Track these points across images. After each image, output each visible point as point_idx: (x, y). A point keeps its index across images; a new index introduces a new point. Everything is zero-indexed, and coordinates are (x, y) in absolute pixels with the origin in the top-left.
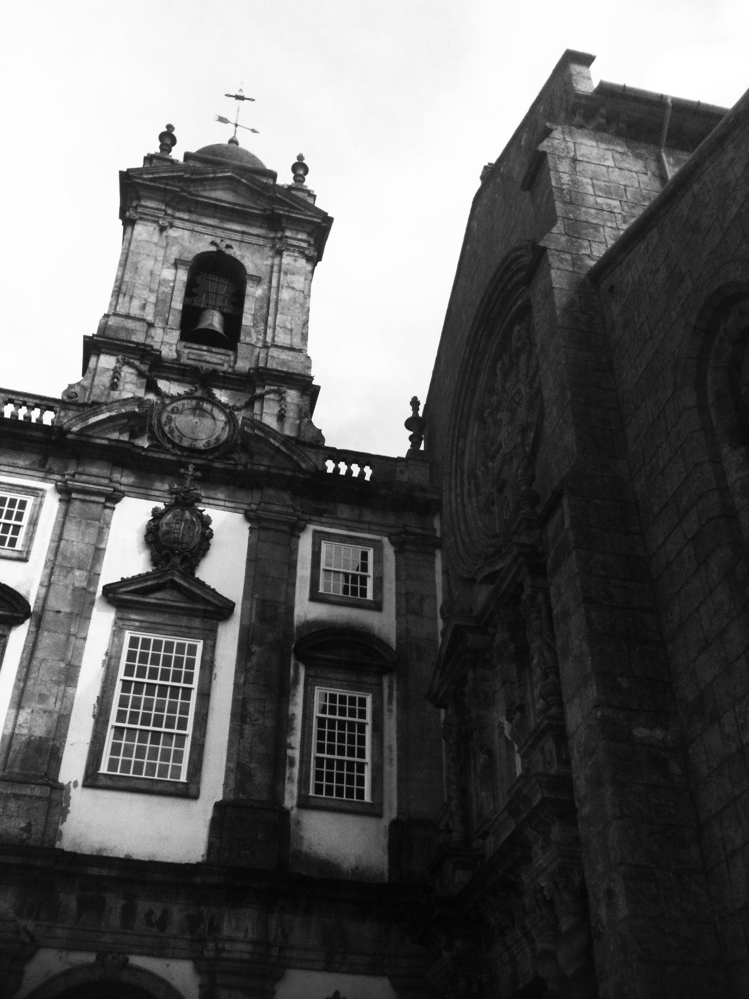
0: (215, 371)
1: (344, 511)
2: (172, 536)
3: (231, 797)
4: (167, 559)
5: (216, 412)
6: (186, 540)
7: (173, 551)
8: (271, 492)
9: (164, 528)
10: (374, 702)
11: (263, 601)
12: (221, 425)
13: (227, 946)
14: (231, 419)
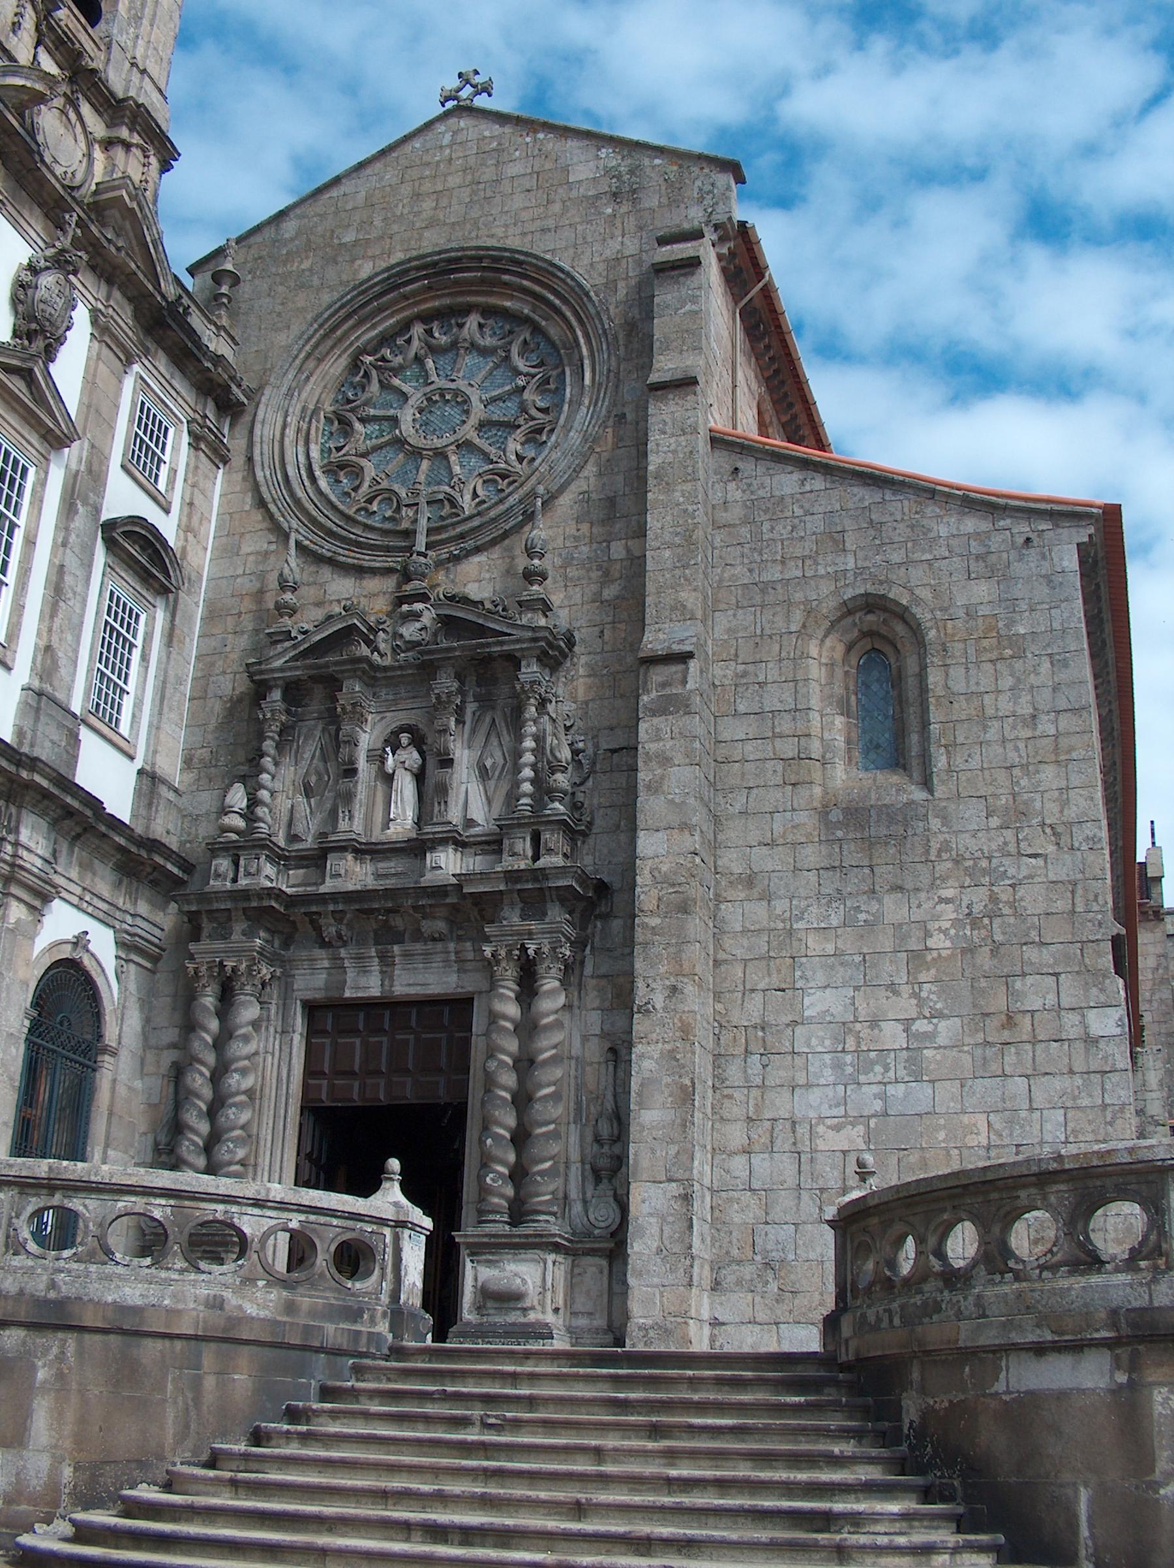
0: (94, 71)
1: (162, 362)
2: (50, 310)
3: (36, 684)
4: (30, 336)
5: (79, 129)
6: (58, 323)
7: (43, 331)
8: (117, 294)
9: (41, 293)
10: (146, 624)
11: (93, 446)
12: (80, 155)
13: (25, 854)
14: (89, 156)
